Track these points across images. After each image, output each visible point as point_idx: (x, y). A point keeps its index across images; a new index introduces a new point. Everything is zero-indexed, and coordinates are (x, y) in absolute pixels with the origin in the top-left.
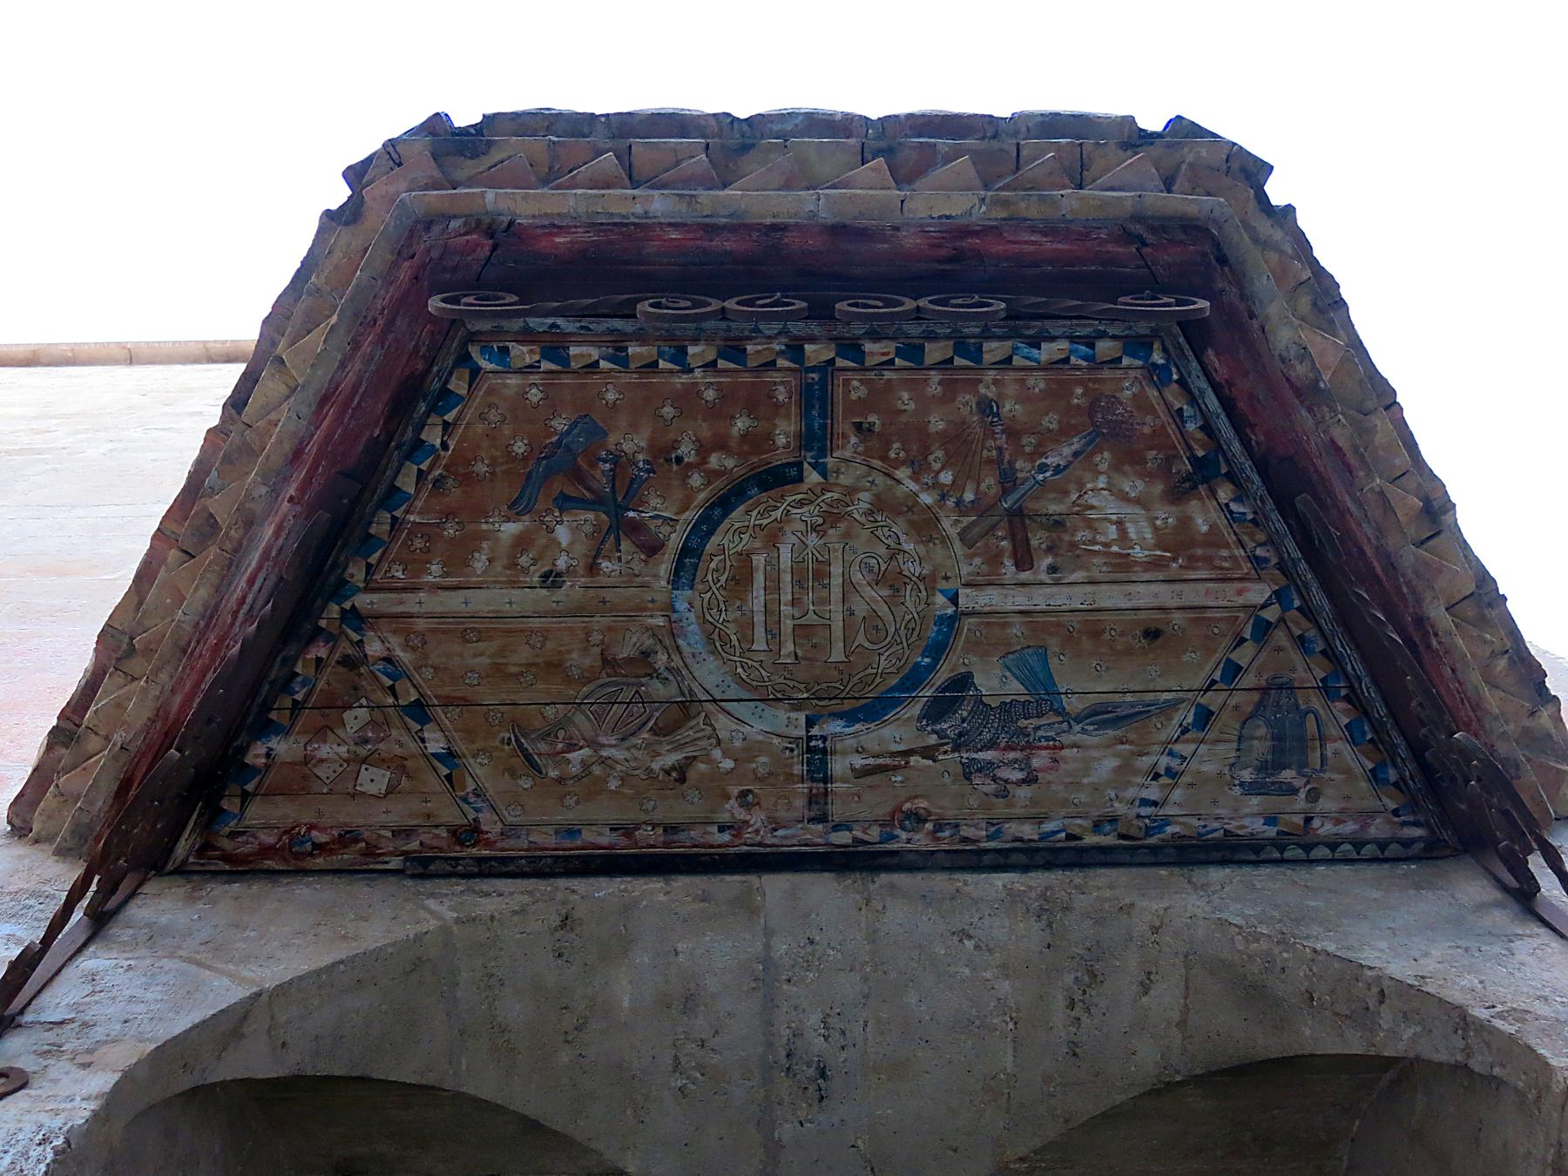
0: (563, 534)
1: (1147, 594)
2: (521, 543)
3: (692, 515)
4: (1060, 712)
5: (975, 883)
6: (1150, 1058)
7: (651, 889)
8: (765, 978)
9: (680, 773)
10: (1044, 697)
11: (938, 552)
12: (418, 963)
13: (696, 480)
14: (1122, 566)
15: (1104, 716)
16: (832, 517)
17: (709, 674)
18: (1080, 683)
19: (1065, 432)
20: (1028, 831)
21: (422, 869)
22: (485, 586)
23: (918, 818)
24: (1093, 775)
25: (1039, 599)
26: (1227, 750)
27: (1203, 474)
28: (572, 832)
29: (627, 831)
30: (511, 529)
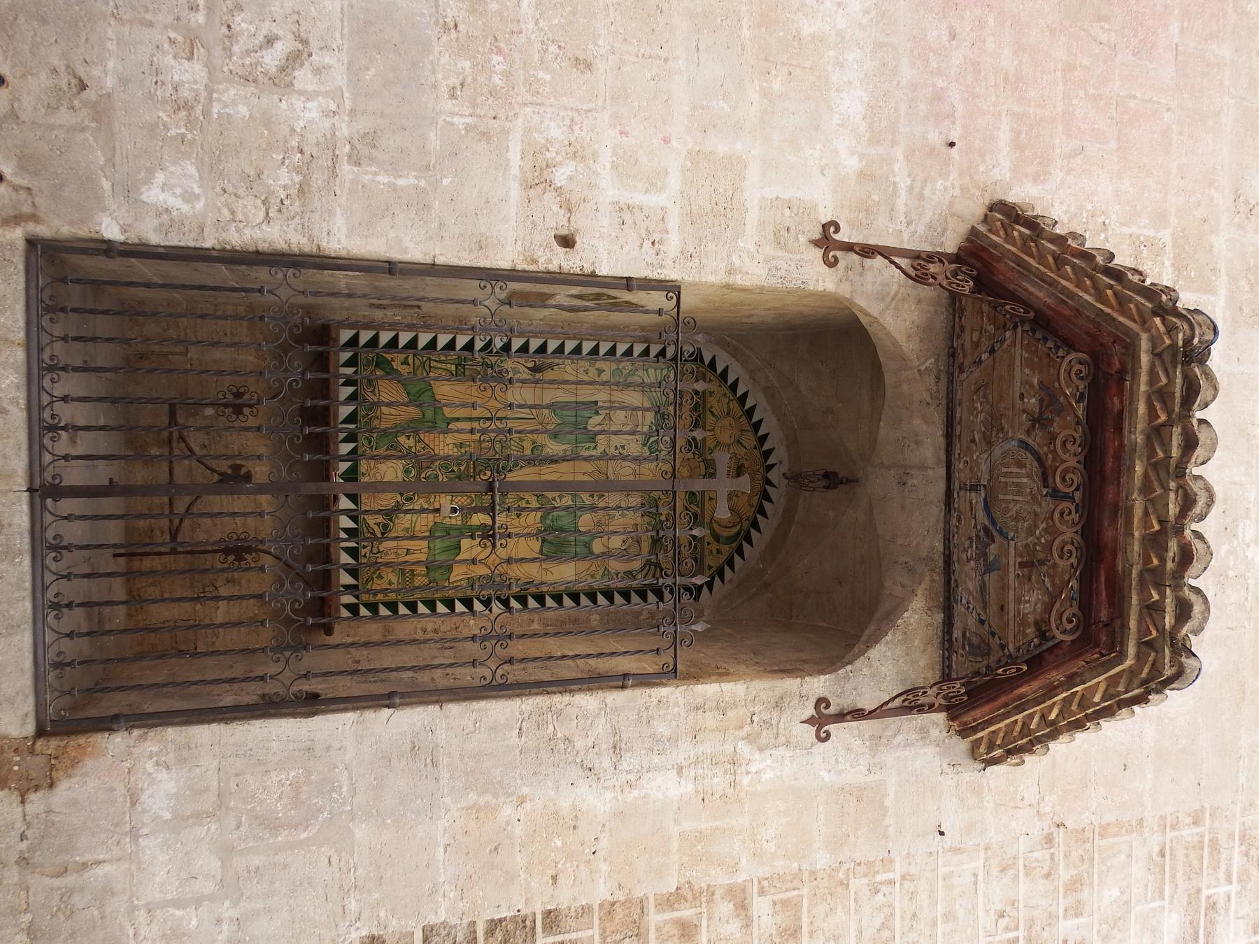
0: (1033, 401)
1: (1012, 606)
2: (1032, 386)
3: (1036, 447)
5: (940, 536)
6: (888, 584)
8: (923, 467)
9: (973, 441)
10: (989, 568)
11: (1023, 535)
13: (1045, 449)
14: (1019, 600)
15: (983, 588)
16: (1034, 498)
17: (997, 451)
18: (992, 579)
19: (1054, 585)
21: (952, 354)
22: (1021, 373)
23: (959, 521)
24: (968, 580)
25: (1011, 570)
26: (973, 629)
28: (960, 404)
29: (960, 423)
30: (1036, 382)
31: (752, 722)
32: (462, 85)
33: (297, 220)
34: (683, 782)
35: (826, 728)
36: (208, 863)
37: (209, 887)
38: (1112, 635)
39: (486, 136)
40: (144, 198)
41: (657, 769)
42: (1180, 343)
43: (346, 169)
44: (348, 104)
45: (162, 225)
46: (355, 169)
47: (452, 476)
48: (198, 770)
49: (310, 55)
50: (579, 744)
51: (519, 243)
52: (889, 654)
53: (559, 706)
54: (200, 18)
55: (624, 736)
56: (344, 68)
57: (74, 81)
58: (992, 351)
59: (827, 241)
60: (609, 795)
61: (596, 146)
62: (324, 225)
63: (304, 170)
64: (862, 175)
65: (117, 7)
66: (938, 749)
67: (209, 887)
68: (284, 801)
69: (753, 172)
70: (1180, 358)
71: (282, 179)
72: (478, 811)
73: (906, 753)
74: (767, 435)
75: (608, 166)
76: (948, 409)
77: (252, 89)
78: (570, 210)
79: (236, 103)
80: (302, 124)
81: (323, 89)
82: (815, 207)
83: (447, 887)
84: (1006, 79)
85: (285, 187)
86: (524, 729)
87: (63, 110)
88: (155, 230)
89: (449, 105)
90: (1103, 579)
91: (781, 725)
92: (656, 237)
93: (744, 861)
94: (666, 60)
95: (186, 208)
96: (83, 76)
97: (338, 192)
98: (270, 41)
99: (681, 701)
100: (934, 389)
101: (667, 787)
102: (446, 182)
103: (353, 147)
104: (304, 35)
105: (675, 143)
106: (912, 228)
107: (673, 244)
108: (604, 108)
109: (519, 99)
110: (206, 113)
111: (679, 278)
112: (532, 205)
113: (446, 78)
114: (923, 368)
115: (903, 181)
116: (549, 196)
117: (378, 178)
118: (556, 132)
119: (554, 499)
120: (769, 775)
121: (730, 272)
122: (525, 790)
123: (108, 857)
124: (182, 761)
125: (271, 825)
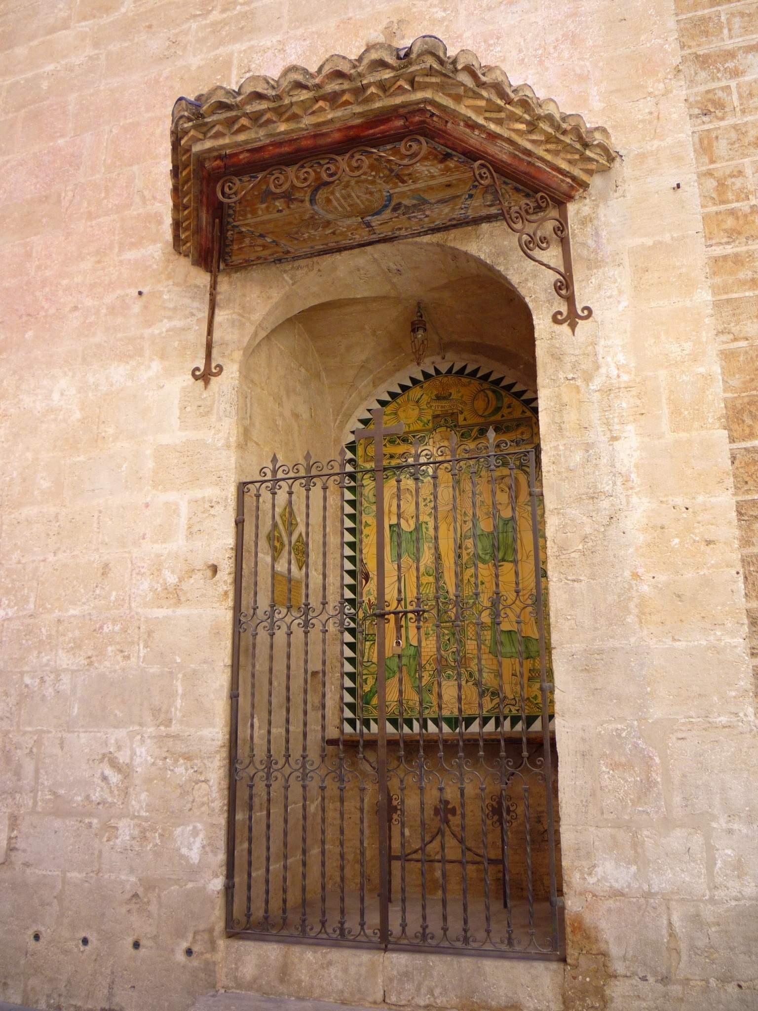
4: (431, 203)
7: (338, 257)
9: (334, 233)
12: (288, 297)
16: (347, 186)
18: (432, 198)
20: (432, 225)
23: (400, 229)
27: (447, 157)
29: (326, 244)
30: (264, 206)
31: (573, 378)
32: (122, 651)
33: (206, 761)
34: (625, 435)
35: (580, 312)
36: (676, 839)
37: (698, 840)
38: (413, 113)
39: (150, 633)
40: (197, 861)
41: (612, 458)
42: (191, 124)
43: (175, 728)
44: (137, 728)
45: (212, 851)
46: (174, 722)
47: (452, 640)
48: (597, 843)
49: (110, 753)
50: (588, 530)
51: (214, 605)
52: (516, 266)
53: (555, 550)
54: (95, 821)
55: (582, 491)
56: (117, 731)
57: (134, 900)
58: (262, 236)
59: (205, 376)
60: (634, 499)
61: (152, 556)
62: (209, 743)
63: (177, 757)
64: (163, 356)
65: (93, 872)
66: (601, 205)
67: (698, 840)
68: (626, 775)
69: (165, 439)
70: (200, 121)
71: (182, 771)
72: (644, 614)
73: (604, 233)
74: (411, 378)
75: (164, 545)
76: (319, 255)
77: (131, 790)
78: (193, 570)
79: (140, 801)
80: (149, 758)
81: (129, 744)
82: (184, 388)
83: (712, 638)
84: (99, 262)
85: (187, 769)
86: (574, 578)
87: (150, 908)
88: (216, 856)
89: (133, 660)
90: (371, 131)
91: (577, 352)
92: (207, 505)
93: (701, 370)
94: (100, 512)
95: (201, 836)
96: (131, 894)
97: (188, 733)
98: (105, 778)
99: (554, 444)
100: (306, 269)
101: (629, 449)
102: (179, 660)
103: (161, 724)
104: (100, 756)
105: (148, 499)
106: (194, 311)
107: (211, 492)
108: (130, 552)
109: (128, 612)
110: (146, 819)
111: (234, 484)
112: (190, 598)
113: (118, 663)
114: (291, 282)
115: (166, 324)
116: (185, 586)
117: (179, 707)
118: (145, 585)
119: (468, 554)
120: (621, 358)
121: (228, 447)
122: (627, 574)
123: (665, 917)
124: (588, 855)
125: (647, 787)
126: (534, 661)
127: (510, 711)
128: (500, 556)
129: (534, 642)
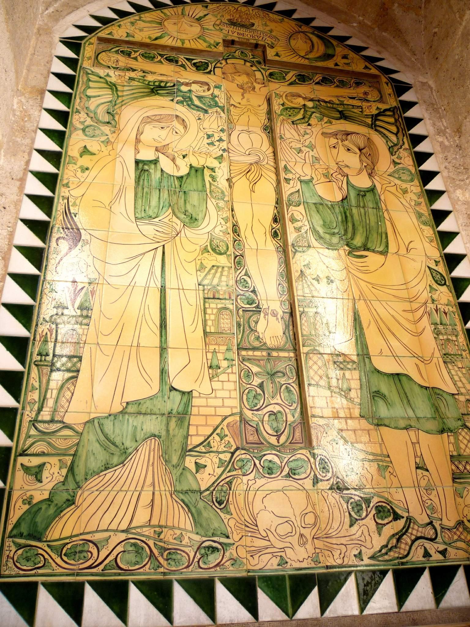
126: (457, 439)
127: (427, 554)
128: (358, 241)
129: (450, 399)
